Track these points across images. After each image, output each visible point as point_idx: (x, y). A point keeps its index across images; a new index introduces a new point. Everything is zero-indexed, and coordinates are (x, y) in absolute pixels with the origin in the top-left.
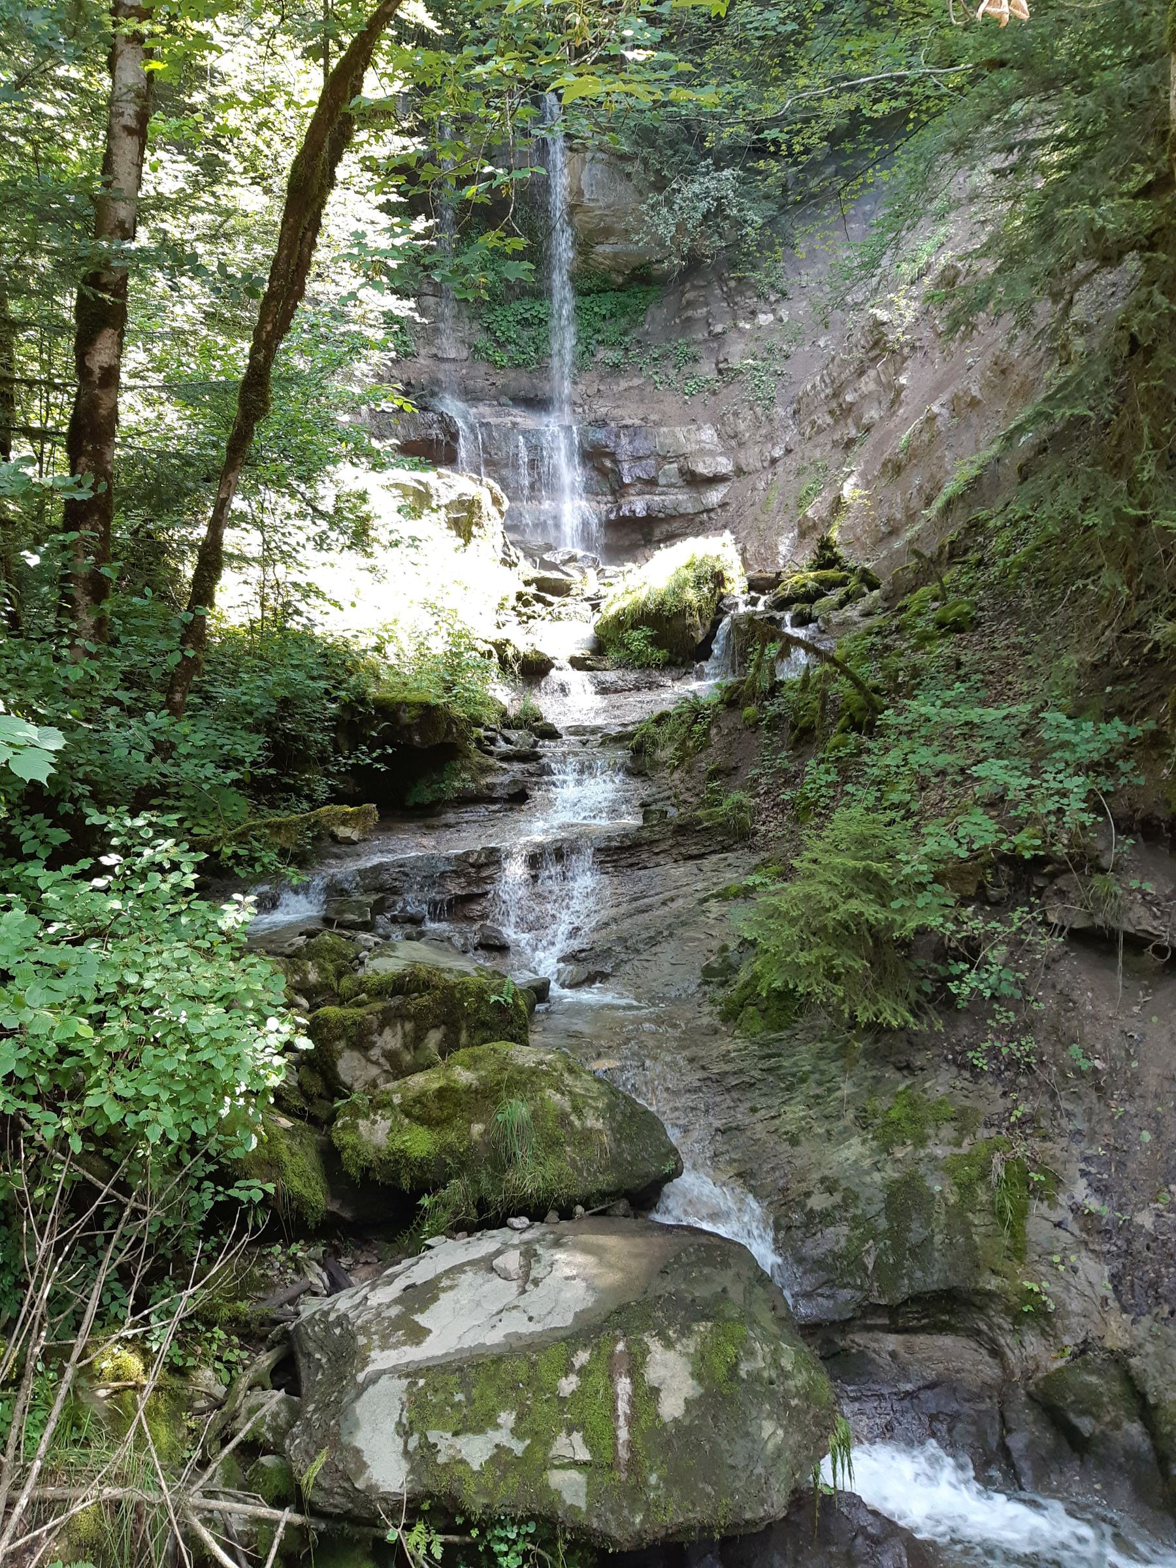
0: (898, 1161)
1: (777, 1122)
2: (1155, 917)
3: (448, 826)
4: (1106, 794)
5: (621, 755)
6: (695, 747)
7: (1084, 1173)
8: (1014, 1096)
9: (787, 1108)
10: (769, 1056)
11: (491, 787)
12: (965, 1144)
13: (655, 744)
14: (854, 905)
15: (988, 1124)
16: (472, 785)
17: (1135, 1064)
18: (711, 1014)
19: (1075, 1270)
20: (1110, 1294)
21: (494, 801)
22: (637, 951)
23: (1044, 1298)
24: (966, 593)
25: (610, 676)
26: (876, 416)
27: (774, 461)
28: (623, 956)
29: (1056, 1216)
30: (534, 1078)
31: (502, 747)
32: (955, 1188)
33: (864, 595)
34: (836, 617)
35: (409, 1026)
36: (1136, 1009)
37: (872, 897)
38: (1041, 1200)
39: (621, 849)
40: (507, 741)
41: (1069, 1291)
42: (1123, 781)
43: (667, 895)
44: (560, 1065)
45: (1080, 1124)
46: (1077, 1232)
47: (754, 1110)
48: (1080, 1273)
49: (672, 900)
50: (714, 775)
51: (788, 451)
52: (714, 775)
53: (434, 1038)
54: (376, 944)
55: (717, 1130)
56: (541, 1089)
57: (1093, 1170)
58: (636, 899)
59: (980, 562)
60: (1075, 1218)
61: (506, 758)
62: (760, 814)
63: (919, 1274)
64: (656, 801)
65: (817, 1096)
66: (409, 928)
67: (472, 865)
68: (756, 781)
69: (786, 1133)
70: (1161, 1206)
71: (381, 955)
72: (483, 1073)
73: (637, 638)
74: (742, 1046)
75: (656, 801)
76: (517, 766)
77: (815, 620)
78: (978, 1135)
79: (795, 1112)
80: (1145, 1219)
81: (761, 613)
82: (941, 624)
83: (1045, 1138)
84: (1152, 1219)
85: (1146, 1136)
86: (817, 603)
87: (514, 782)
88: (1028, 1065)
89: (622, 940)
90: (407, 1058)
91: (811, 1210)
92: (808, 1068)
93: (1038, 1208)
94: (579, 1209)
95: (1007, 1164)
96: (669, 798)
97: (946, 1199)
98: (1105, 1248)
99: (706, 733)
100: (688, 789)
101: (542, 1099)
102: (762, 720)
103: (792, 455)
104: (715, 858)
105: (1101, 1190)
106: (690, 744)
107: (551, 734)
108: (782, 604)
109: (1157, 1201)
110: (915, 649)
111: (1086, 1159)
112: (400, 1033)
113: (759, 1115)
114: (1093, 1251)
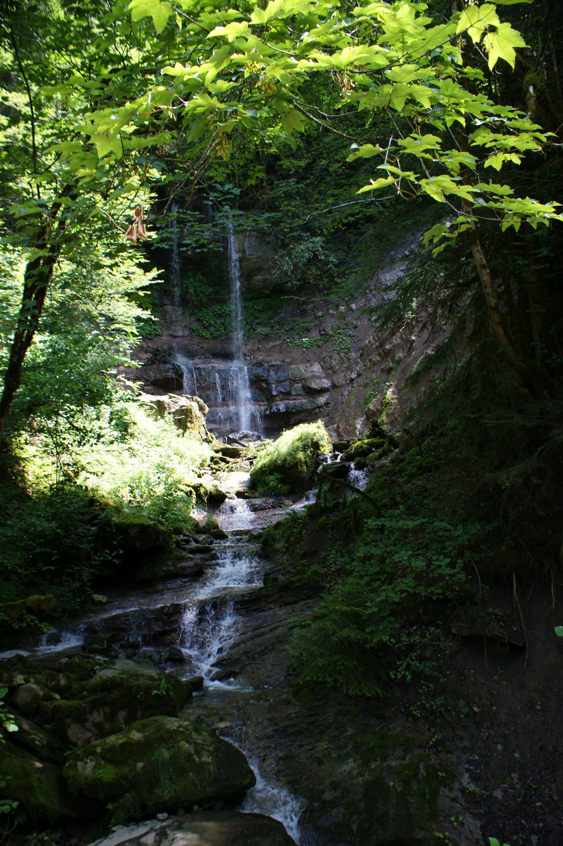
0: (371, 770)
1: (312, 752)
2: (502, 627)
3: (157, 592)
4: (476, 562)
5: (254, 547)
6: (294, 541)
7: (467, 770)
8: (433, 730)
9: (319, 744)
10: (312, 715)
11: (184, 568)
12: (407, 758)
13: (274, 540)
14: (345, 632)
15: (420, 747)
16: (172, 568)
17: (494, 708)
18: (287, 693)
19: (463, 824)
20: (480, 837)
21: (185, 576)
22: (254, 659)
23: (447, 841)
24: (434, 450)
25: (258, 502)
26: (402, 356)
27: (352, 380)
28: (246, 662)
29: (452, 795)
30: (175, 736)
31: (194, 545)
32: (401, 783)
33: (392, 451)
34: (377, 464)
35: (107, 709)
36: (495, 678)
37: (355, 626)
38: (445, 787)
39: (249, 601)
40: (197, 541)
41: (460, 837)
42: (483, 555)
43: (273, 626)
44: (190, 728)
45: (466, 743)
46: (463, 803)
47: (301, 746)
48: (466, 826)
49: (275, 628)
50: (303, 556)
51: (359, 375)
52: (303, 556)
53: (122, 715)
54: (105, 661)
55: (280, 758)
56: (179, 741)
57: (472, 768)
58: (256, 629)
59: (441, 434)
60: (462, 795)
61: (193, 551)
62: (327, 577)
63: (381, 832)
64: (273, 572)
65: (335, 736)
66: (129, 651)
67: (165, 614)
68: (325, 558)
69: (316, 758)
70: (506, 786)
71: (106, 668)
72: (147, 734)
73: (272, 480)
74: (298, 710)
75: (273, 572)
76: (198, 556)
77: (367, 466)
78: (415, 753)
79: (323, 745)
80: (498, 794)
81: (338, 463)
82: (420, 468)
83: (448, 752)
84: (501, 794)
85: (500, 747)
86: (368, 457)
87: (196, 565)
88: (441, 712)
89: (246, 653)
90: (107, 726)
91: (325, 800)
92: (331, 721)
93: (445, 791)
94: (196, 807)
95: (426, 767)
96: (280, 570)
97: (396, 790)
98: (477, 811)
99: (300, 533)
100: (290, 565)
101: (178, 747)
102: (328, 524)
103: (361, 377)
104: (301, 603)
105: (475, 779)
106: (292, 539)
107: (222, 536)
108: (349, 458)
109: (504, 783)
110: (406, 482)
111: (469, 762)
112: (102, 713)
113: (303, 749)
114: (472, 813)
